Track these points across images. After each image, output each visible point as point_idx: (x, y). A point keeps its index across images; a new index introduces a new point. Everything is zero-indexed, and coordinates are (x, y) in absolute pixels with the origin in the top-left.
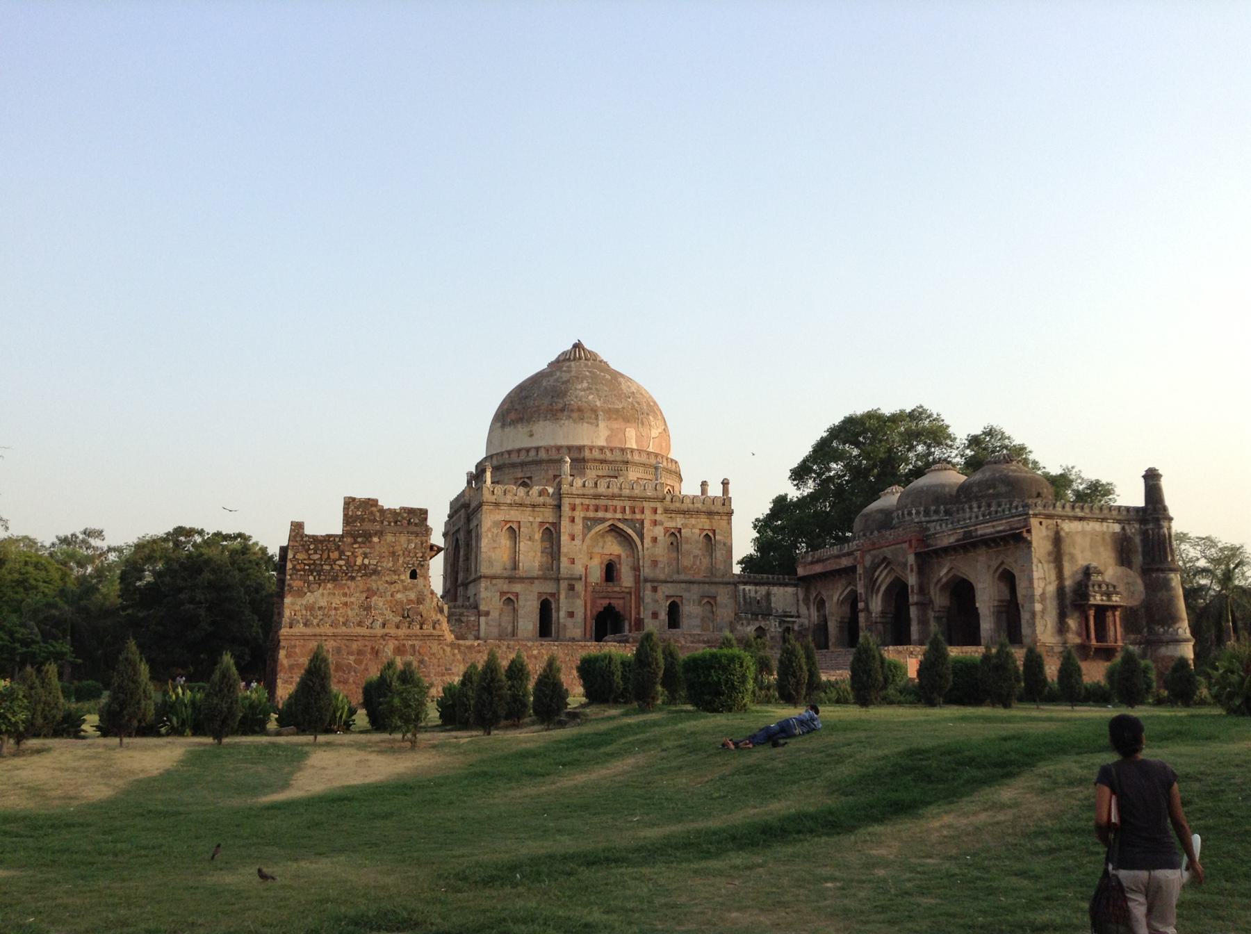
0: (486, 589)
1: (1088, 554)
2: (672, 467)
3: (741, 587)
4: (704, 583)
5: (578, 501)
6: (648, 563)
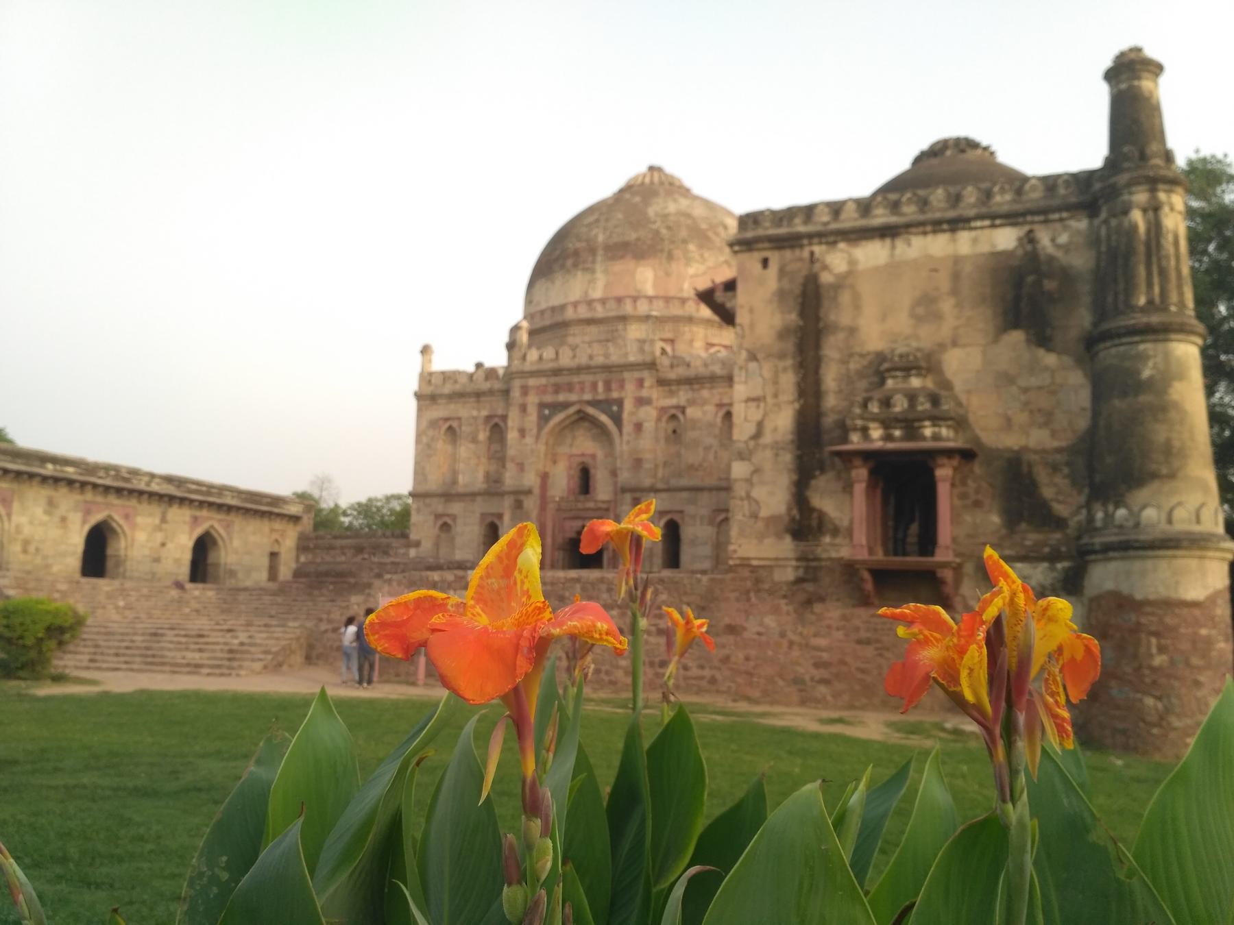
0: (418, 511)
1: (901, 322)
5: (532, 382)
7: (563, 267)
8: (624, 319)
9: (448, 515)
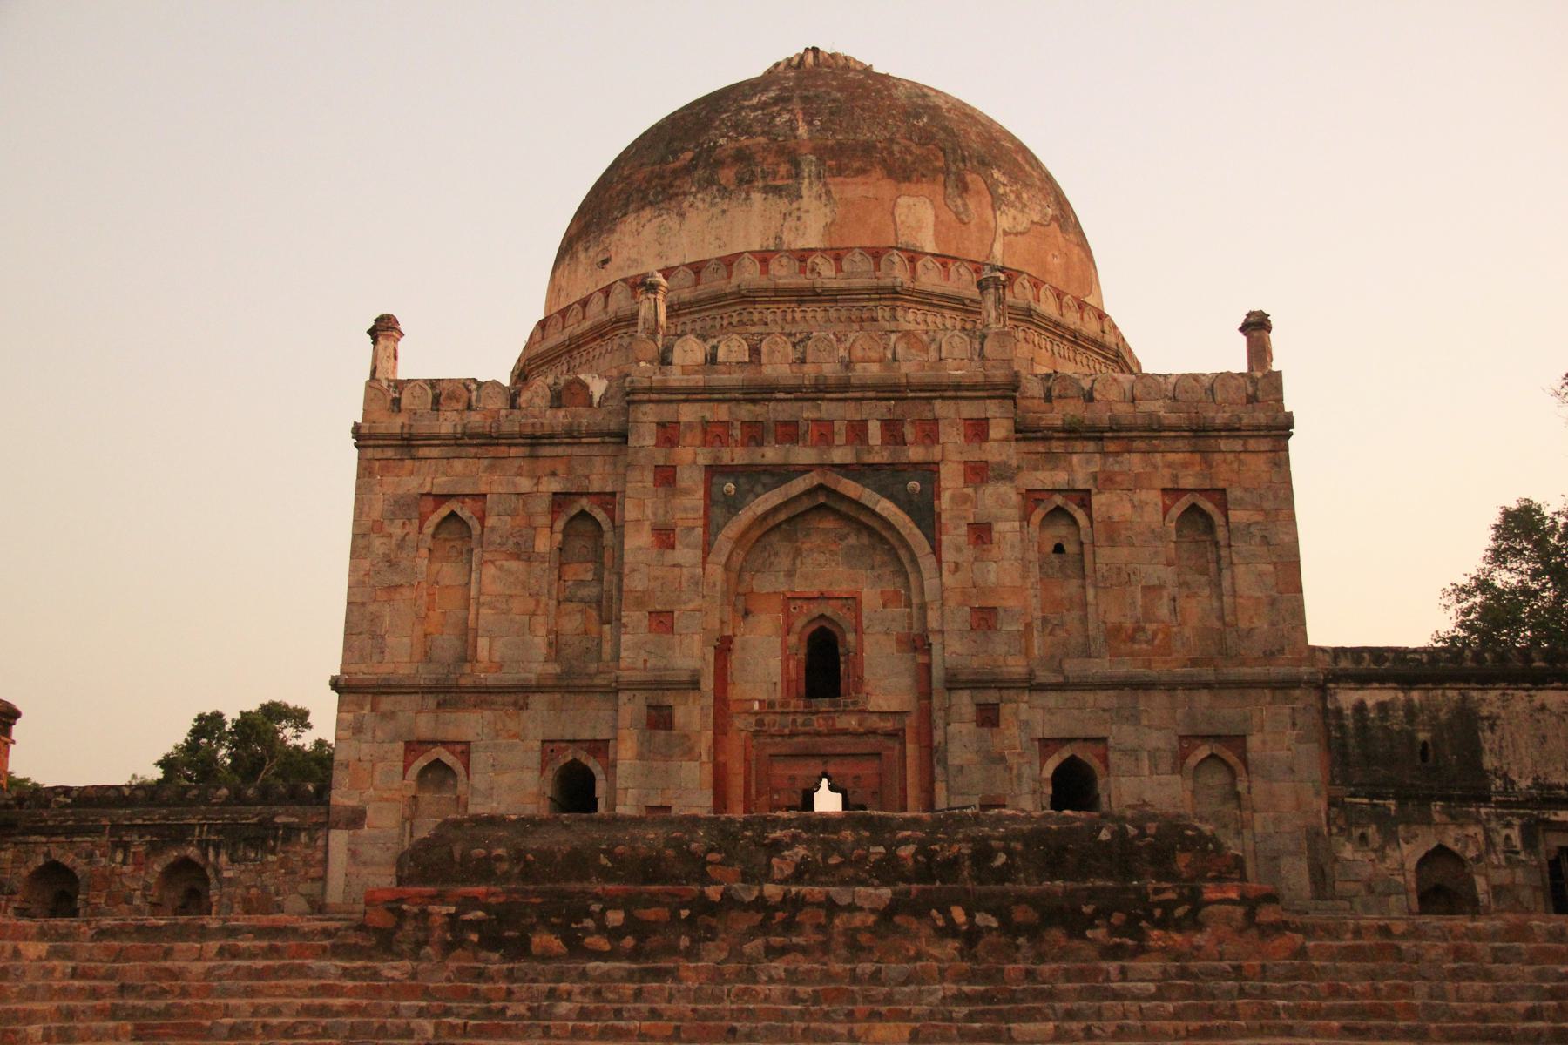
2: (1091, 327)
3: (1347, 698)
4: (1192, 685)
5: (688, 413)
6: (959, 619)
7: (711, 181)
8: (892, 294)
9: (444, 743)
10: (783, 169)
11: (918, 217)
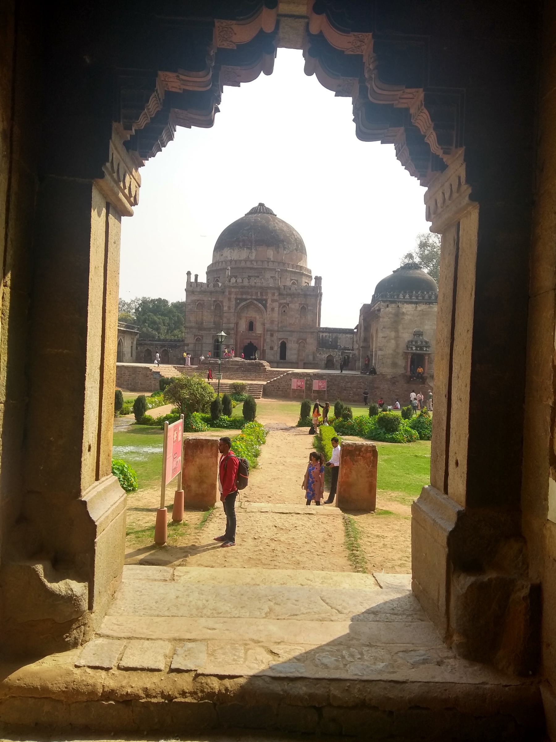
3: (321, 334)
4: (300, 332)
5: (233, 290)
10: (250, 244)
11: (270, 253)
